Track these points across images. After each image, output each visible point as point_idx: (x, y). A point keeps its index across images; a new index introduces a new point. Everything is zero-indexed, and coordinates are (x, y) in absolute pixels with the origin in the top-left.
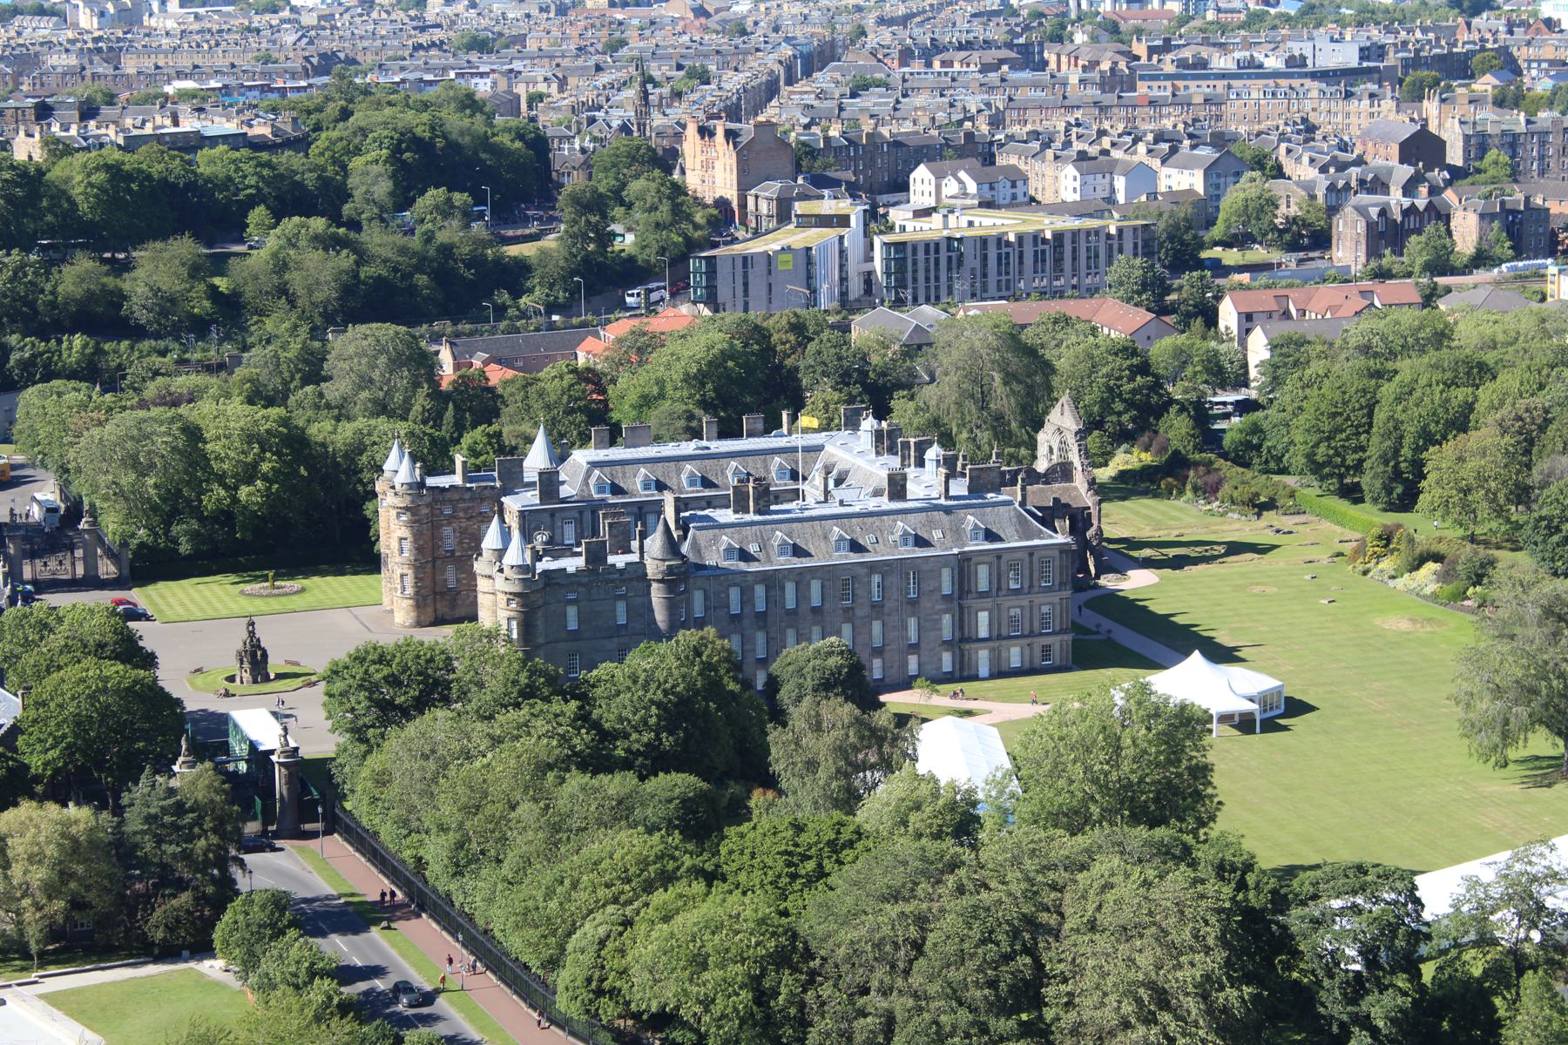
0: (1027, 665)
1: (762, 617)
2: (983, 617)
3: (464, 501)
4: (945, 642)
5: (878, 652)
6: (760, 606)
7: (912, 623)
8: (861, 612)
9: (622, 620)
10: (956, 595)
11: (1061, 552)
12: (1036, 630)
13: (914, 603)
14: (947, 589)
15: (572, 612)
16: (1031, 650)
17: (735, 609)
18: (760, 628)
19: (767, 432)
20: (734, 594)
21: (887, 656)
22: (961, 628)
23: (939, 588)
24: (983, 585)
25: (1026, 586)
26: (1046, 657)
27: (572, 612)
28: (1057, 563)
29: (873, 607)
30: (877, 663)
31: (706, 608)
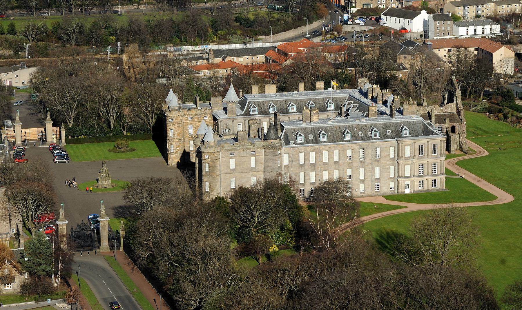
1: (314, 165)
2: (408, 168)
3: (197, 114)
6: (312, 161)
7: (377, 169)
9: (253, 165)
10: (396, 158)
13: (378, 161)
14: (392, 156)
15: (232, 161)
17: (302, 161)
18: (313, 170)
19: (326, 88)
20: (302, 155)
21: (366, 182)
22: (398, 172)
23: (389, 155)
24: (408, 155)
25: (426, 154)
27: (232, 161)
28: (439, 145)
30: (362, 187)
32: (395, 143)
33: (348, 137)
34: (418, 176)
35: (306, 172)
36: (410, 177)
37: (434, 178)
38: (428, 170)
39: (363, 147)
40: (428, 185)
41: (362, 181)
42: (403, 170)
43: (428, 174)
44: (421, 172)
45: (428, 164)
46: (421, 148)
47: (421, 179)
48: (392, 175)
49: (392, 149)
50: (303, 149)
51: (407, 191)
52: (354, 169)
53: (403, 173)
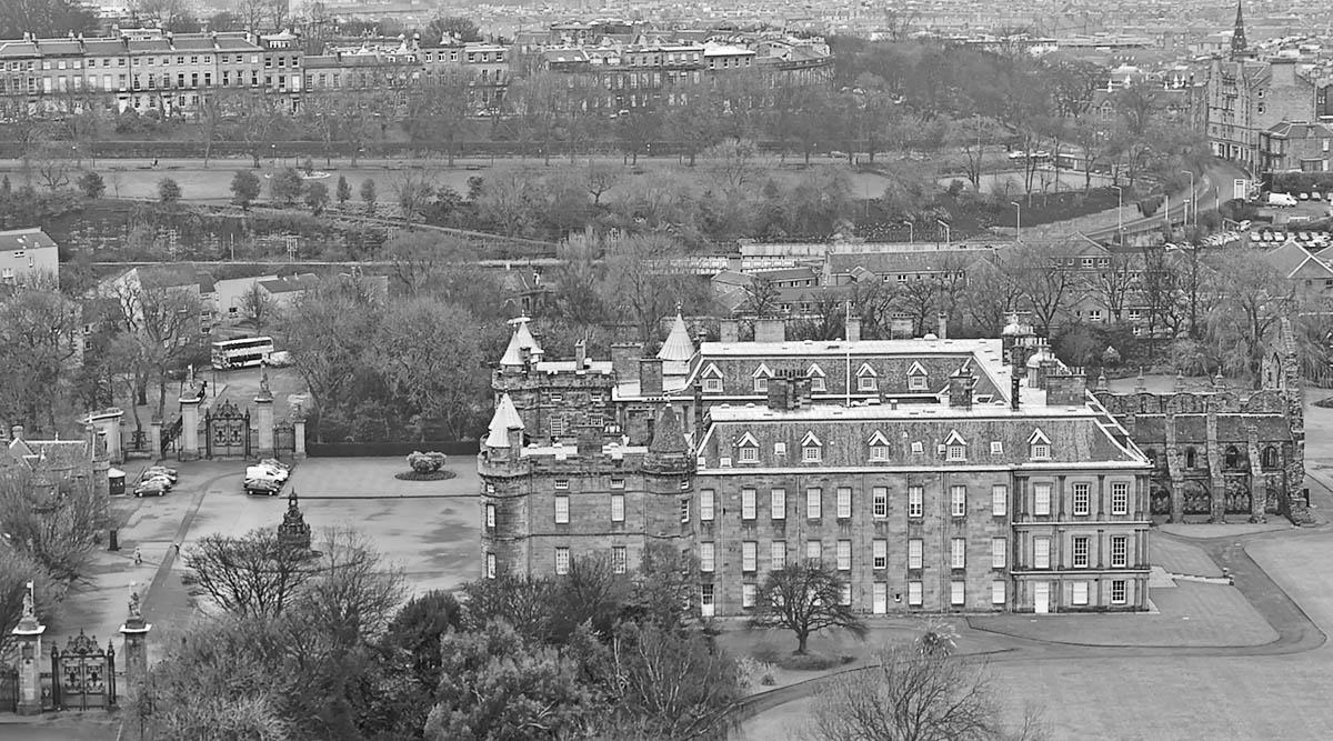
0: (1094, 603)
1: (781, 523)
3: (574, 389)
4: (995, 569)
5: (915, 575)
6: (778, 514)
7: (958, 547)
8: (898, 527)
10: (1010, 516)
11: (1138, 477)
12: (1106, 565)
13: (959, 522)
17: (749, 514)
19: (919, 334)
20: (749, 499)
21: (927, 579)
22: (1016, 554)
25: (1095, 511)
26: (1118, 595)
28: (1133, 489)
29: (910, 523)
32: (1006, 478)
33: (879, 455)
35: (761, 541)
38: (1100, 553)
39: (917, 483)
41: (915, 575)
42: (1030, 550)
43: (1100, 565)
45: (1100, 538)
52: (892, 539)
53: (1030, 558)
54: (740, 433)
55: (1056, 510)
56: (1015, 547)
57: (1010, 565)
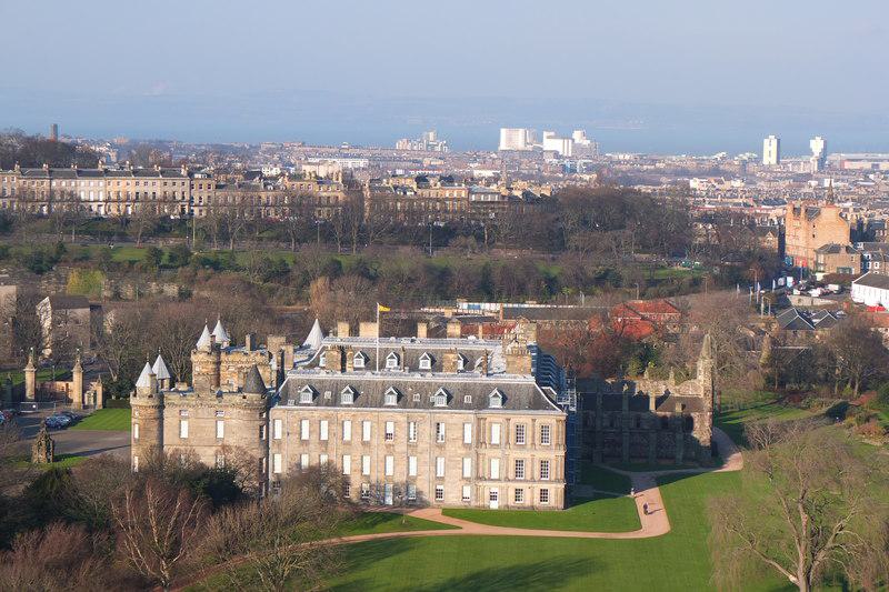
2: (495, 464)
7: (441, 461)
10: (474, 445)
14: (468, 439)
16: (532, 492)
22: (478, 469)
25: (529, 443)
27: (185, 424)
28: (554, 429)
31: (283, 433)
34: (514, 480)
36: (499, 480)
37: (545, 486)
38: (532, 471)
40: (530, 498)
43: (532, 478)
44: (518, 473)
46: (519, 430)
47: (519, 486)
48: (467, 474)
49: (468, 428)
50: (307, 414)
51: (494, 505)
54: (302, 385)
55: (504, 442)
56: (478, 464)
57: (474, 475)
